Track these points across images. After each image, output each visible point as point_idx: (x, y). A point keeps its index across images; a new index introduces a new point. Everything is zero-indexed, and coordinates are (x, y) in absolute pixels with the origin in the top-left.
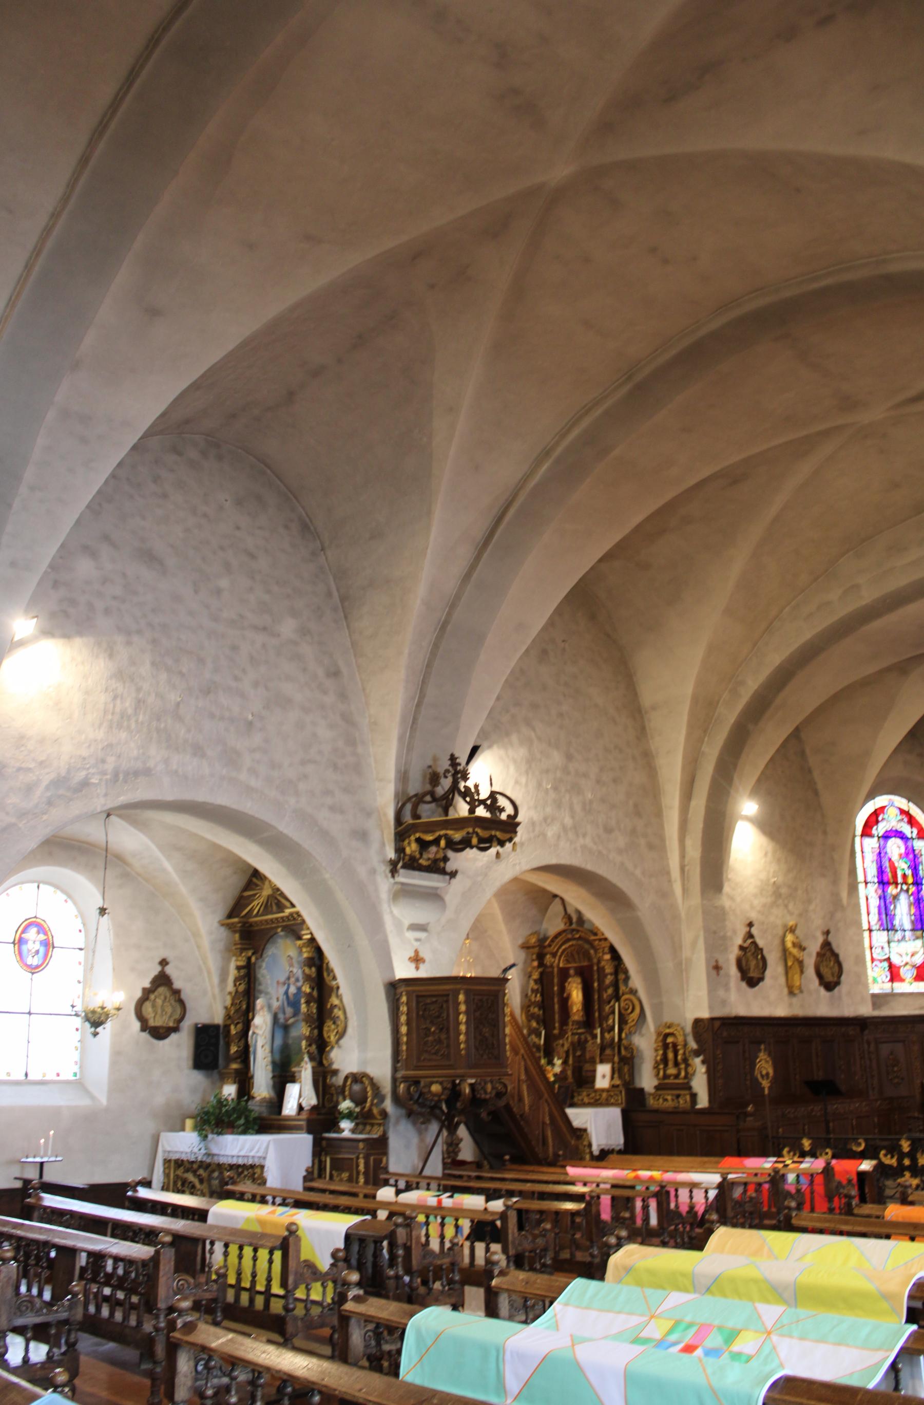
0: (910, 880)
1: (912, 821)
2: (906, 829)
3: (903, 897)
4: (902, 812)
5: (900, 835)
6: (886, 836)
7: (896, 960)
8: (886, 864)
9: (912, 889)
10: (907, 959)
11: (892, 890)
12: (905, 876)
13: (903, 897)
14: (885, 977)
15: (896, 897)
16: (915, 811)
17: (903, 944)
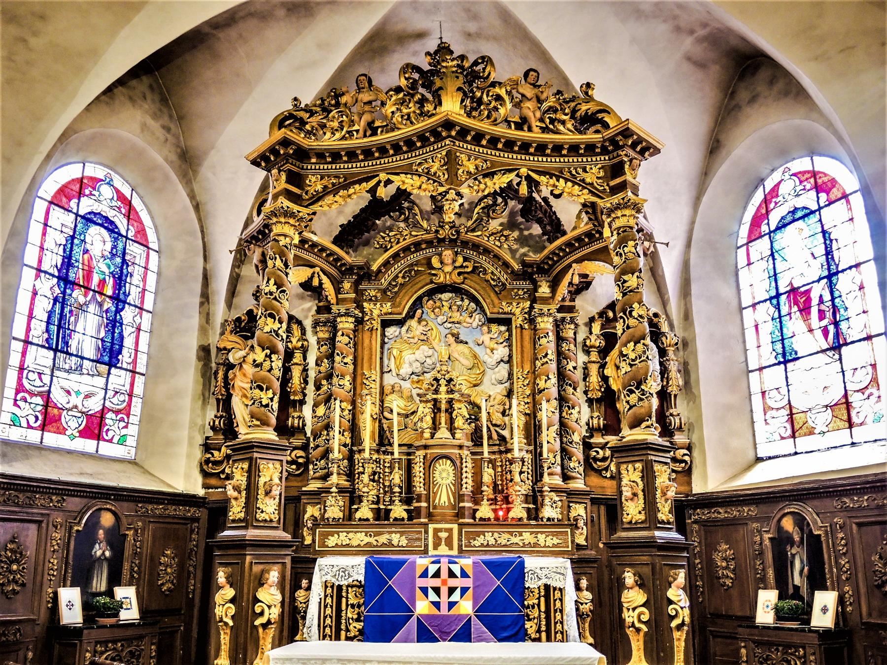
0: (109, 291)
1: (131, 213)
2: (121, 223)
3: (92, 308)
4: (121, 197)
5: (109, 225)
6: (89, 219)
7: (58, 397)
8: (77, 252)
9: (108, 304)
10: (75, 400)
11: (78, 295)
12: (102, 282)
13: (92, 308)
14: (34, 419)
15: (81, 308)
16: (137, 203)
17: (74, 377)
